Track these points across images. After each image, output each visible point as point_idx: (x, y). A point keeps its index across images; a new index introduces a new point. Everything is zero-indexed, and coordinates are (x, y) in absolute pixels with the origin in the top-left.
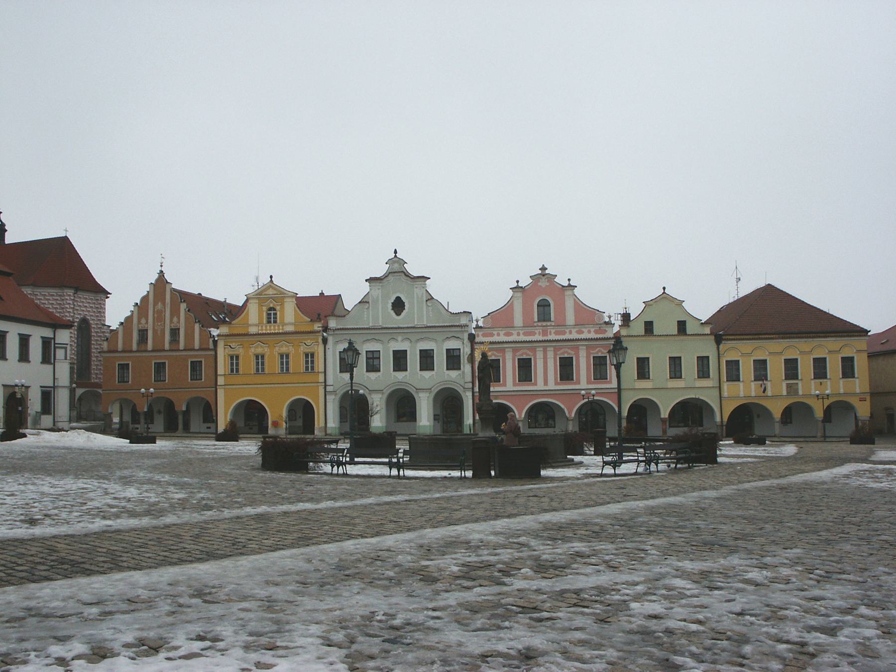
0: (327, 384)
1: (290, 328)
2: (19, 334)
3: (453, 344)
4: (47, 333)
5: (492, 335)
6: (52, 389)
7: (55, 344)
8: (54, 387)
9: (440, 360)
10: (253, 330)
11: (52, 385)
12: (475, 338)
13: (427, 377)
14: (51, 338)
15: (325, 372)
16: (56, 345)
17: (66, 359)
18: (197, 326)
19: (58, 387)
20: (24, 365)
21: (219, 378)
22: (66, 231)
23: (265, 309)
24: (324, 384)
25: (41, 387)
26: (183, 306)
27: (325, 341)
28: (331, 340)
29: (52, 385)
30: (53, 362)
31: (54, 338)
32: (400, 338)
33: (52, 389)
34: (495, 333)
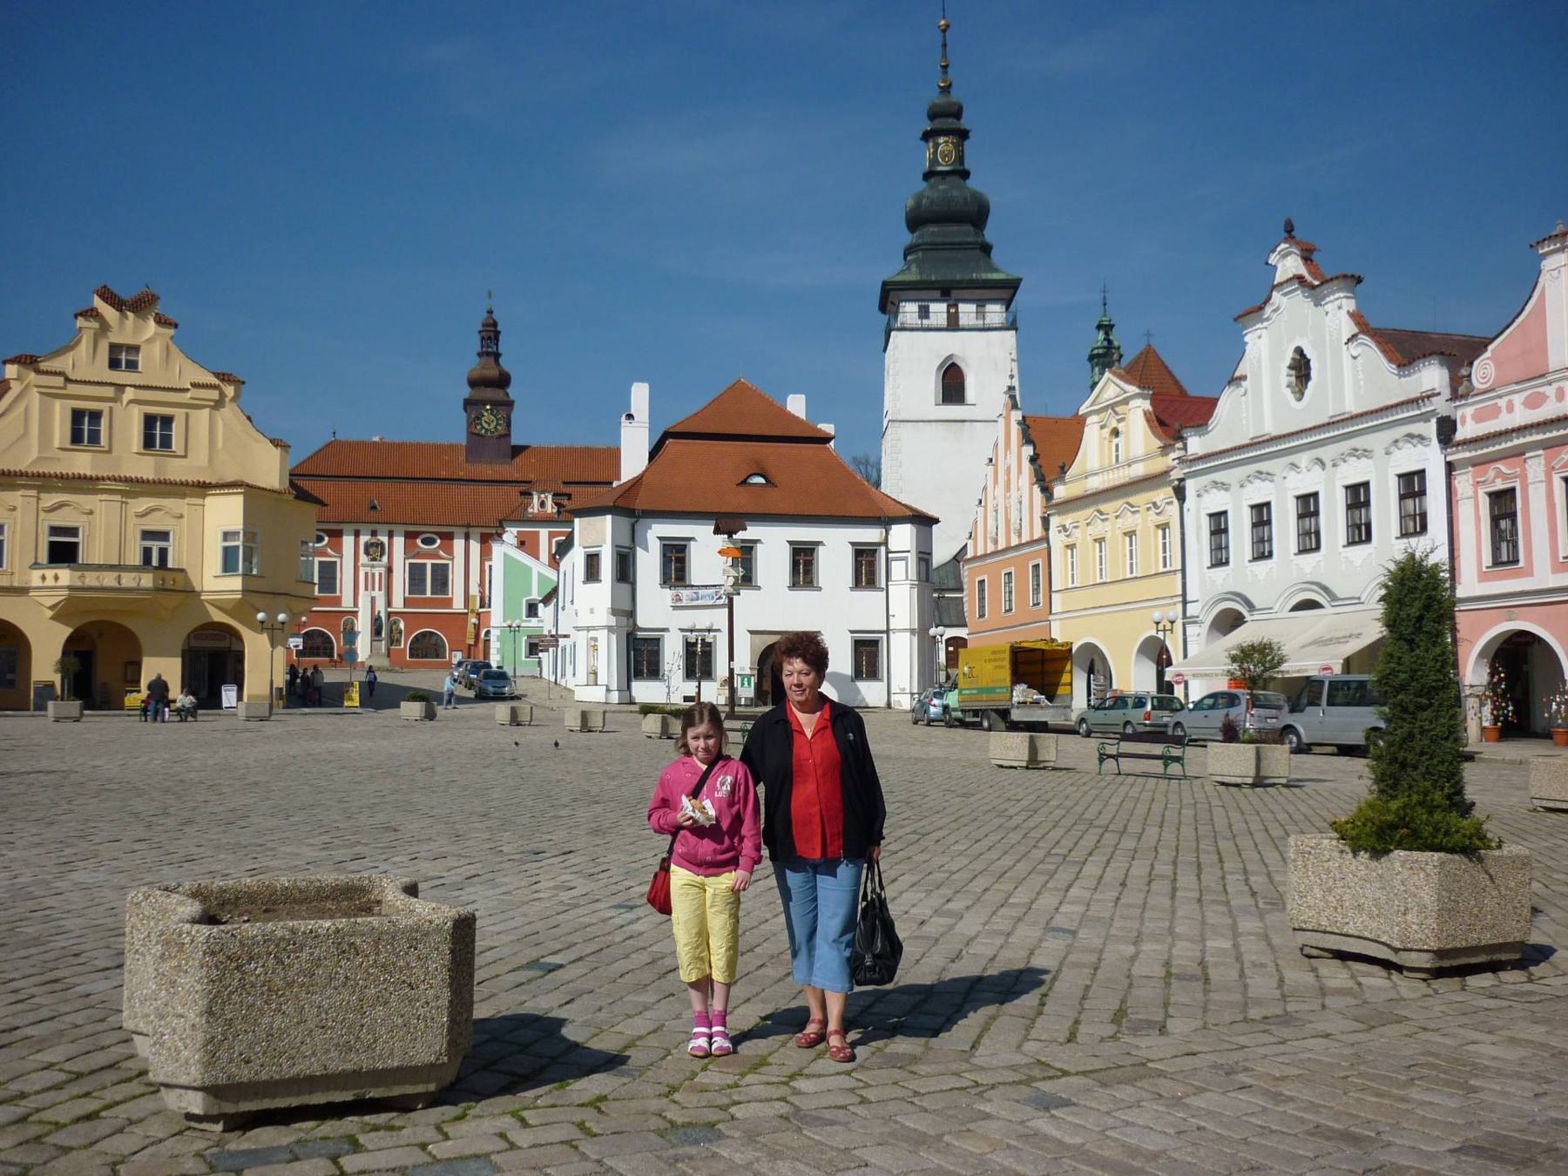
0: (1189, 598)
1: (1139, 470)
2: (790, 543)
3: (1408, 458)
4: (871, 535)
5: (1495, 412)
6: (885, 636)
7: (888, 552)
8: (887, 632)
9: (1385, 510)
10: (1095, 484)
11: (885, 628)
12: (1454, 430)
13: (1358, 563)
14: (879, 544)
15: (1183, 570)
16: (890, 555)
17: (907, 579)
18: (1036, 489)
19: (895, 630)
20: (803, 595)
21: (1053, 595)
22: (1149, 335)
23: (1106, 432)
24: (1180, 599)
25: (852, 632)
26: (1028, 451)
27: (1180, 493)
28: (1191, 486)
29: (885, 628)
30: (883, 585)
31: (886, 543)
32: (1303, 459)
33: (885, 636)
34: (1502, 403)
